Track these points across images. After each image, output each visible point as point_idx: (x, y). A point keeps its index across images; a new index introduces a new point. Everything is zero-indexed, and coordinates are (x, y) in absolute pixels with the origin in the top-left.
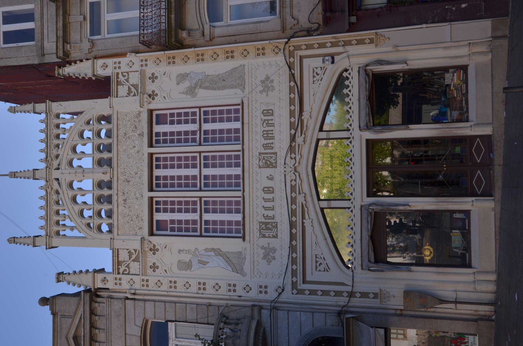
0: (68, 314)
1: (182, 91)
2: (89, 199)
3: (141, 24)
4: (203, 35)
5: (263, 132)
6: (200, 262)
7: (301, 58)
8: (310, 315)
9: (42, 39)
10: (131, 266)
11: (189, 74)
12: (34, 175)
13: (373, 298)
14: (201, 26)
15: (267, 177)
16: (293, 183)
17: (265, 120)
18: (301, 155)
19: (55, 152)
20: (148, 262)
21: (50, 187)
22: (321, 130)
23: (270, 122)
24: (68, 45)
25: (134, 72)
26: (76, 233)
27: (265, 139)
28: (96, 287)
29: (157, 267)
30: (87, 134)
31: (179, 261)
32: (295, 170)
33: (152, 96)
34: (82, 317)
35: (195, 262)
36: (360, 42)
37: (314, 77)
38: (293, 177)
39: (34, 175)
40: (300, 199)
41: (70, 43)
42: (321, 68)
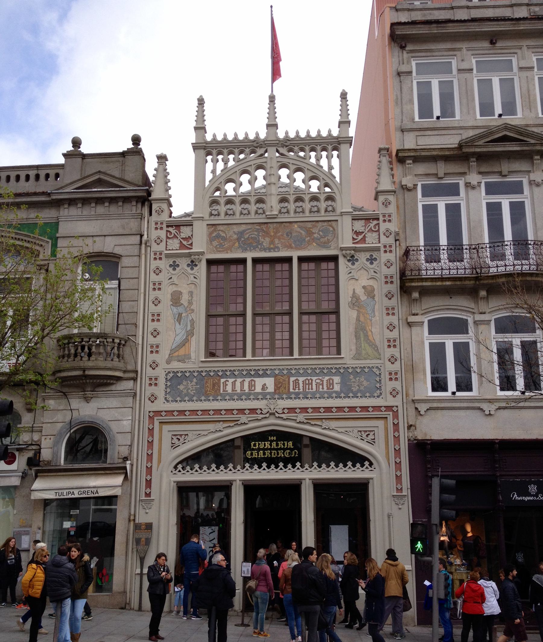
0: (123, 169)
1: (356, 292)
4: (414, 315)
5: (311, 379)
6: (180, 315)
11: (374, 299)
12: (272, 126)
13: (146, 493)
14: (424, 312)
15: (265, 384)
16: (259, 411)
17: (323, 381)
20: (179, 259)
21: (258, 144)
22: (311, 439)
23: (321, 387)
24: (411, 162)
25: (379, 238)
26: (209, 176)
27: (303, 381)
28: (152, 202)
29: (174, 269)
30: (314, 185)
31: (181, 293)
32: (271, 414)
33: (352, 259)
34: (121, 189)
35: (181, 309)
36: (399, 478)
37: (366, 431)
38: (265, 411)
39: (272, 126)
40: (243, 419)
41: (413, 162)
42: (374, 439)
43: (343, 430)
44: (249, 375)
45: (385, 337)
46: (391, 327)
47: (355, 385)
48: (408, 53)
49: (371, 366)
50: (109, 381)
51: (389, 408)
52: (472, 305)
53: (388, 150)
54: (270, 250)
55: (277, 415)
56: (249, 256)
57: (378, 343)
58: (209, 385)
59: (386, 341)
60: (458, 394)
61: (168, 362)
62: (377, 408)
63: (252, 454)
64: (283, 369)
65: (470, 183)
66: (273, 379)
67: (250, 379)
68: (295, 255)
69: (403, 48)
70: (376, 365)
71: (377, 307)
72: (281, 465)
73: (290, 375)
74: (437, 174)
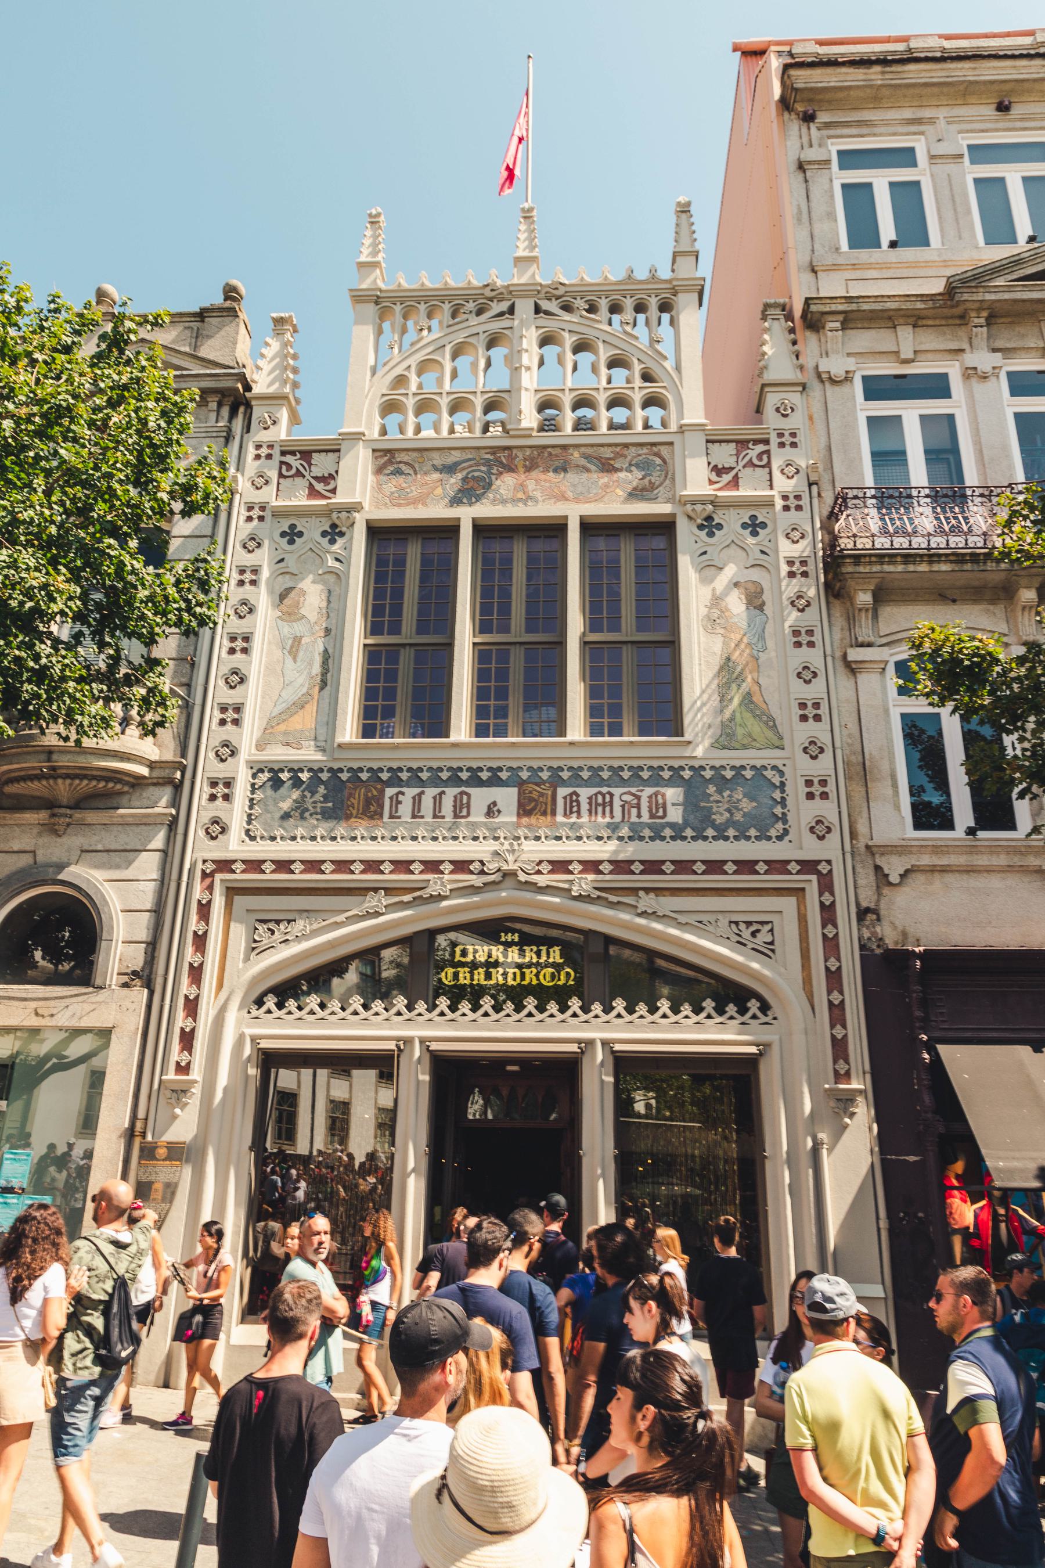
2: (462, 385)
3: (891, 492)
4: (862, 645)
5: (609, 793)
6: (297, 640)
7: (799, 892)
8: (148, 906)
9: (854, 266)
10: (299, 480)
11: (762, 610)
13: (178, 1063)
14: (884, 640)
15: (495, 804)
16: (475, 867)
17: (638, 798)
18: (548, 887)
19: (580, 304)
21: (494, 294)
24: (838, 325)
25: (771, 480)
27: (590, 798)
28: (253, 403)
29: (291, 542)
30: (619, 375)
33: (709, 525)
35: (299, 628)
36: (840, 1048)
37: (749, 924)
38: (492, 866)
40: (437, 884)
41: (843, 329)
42: (772, 943)
43: (691, 919)
44: (455, 780)
45: (793, 697)
46: (806, 674)
47: (721, 810)
48: (819, 129)
49: (758, 763)
50: (111, 785)
51: (808, 866)
52: (1003, 628)
53: (783, 308)
54: (515, 501)
55: (522, 877)
56: (466, 515)
57: (775, 712)
58: (355, 802)
59: (795, 706)
60: (981, 834)
61: (260, 747)
62: (777, 866)
63: (456, 976)
64: (541, 769)
65: (975, 369)
66: (515, 790)
67: (458, 790)
68: (574, 513)
69: (808, 118)
70: (773, 762)
71: (769, 629)
72: (530, 1003)
73: (556, 781)
74: (897, 353)
